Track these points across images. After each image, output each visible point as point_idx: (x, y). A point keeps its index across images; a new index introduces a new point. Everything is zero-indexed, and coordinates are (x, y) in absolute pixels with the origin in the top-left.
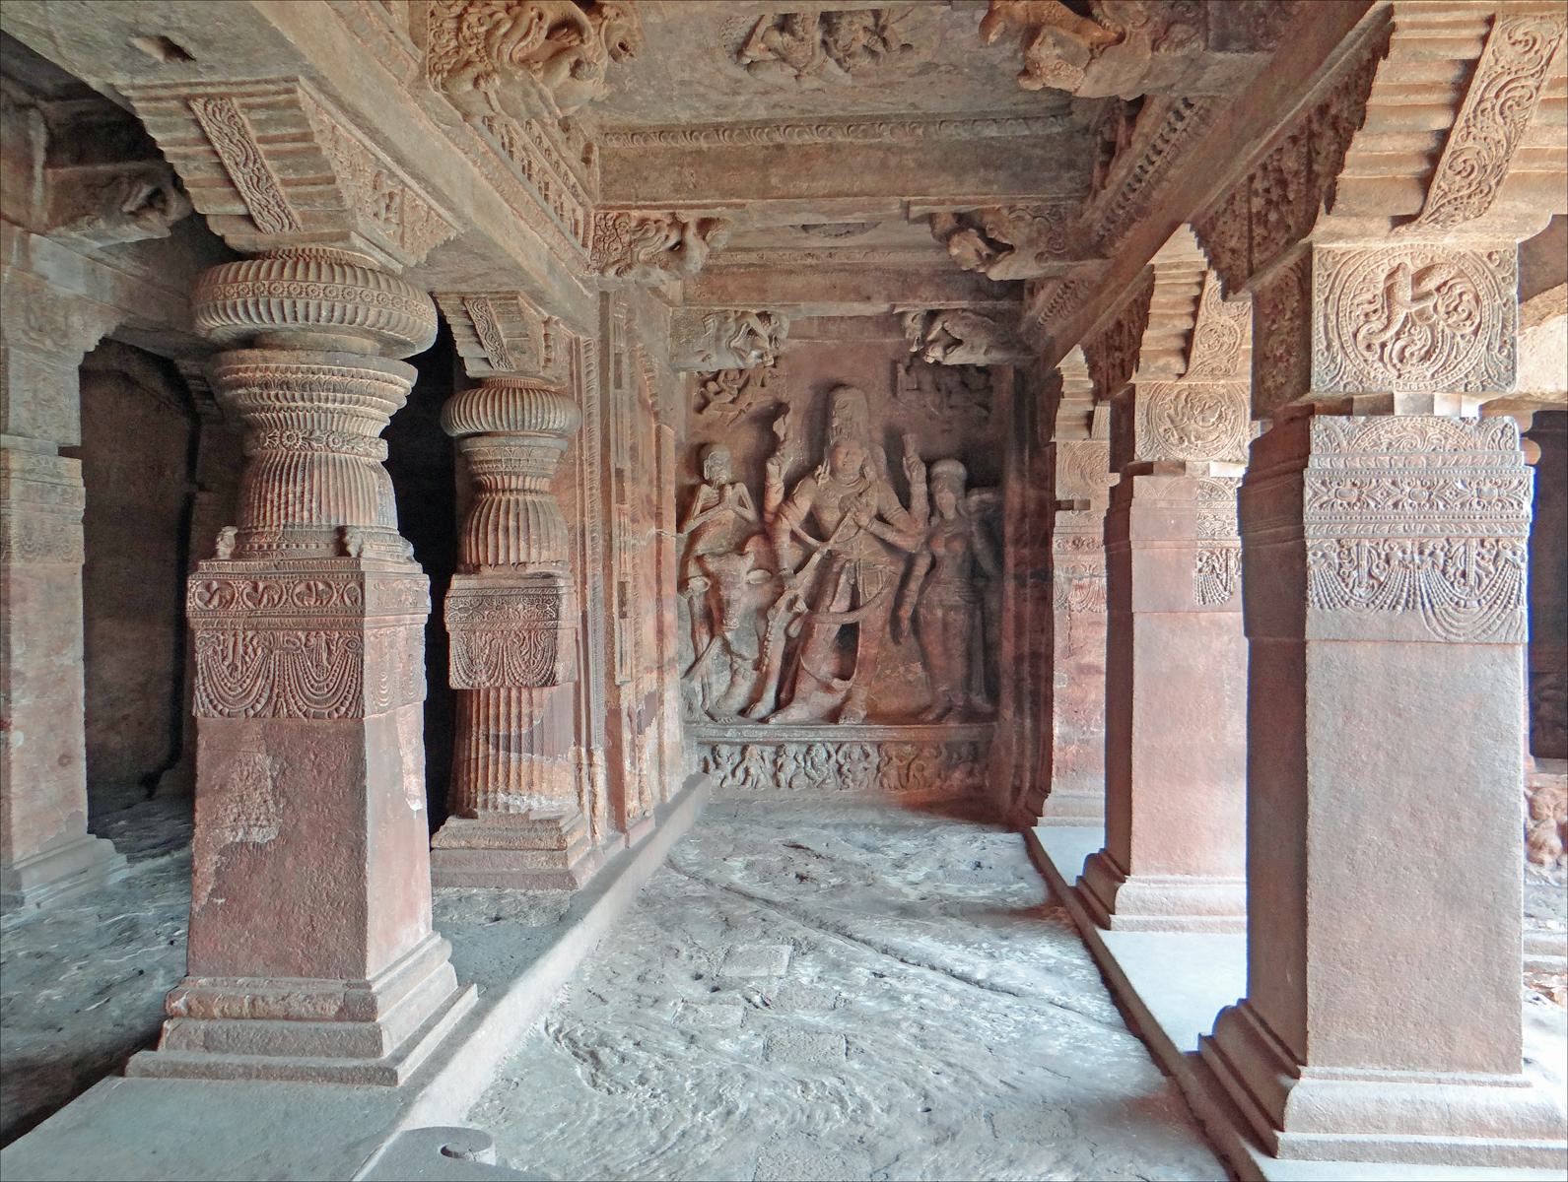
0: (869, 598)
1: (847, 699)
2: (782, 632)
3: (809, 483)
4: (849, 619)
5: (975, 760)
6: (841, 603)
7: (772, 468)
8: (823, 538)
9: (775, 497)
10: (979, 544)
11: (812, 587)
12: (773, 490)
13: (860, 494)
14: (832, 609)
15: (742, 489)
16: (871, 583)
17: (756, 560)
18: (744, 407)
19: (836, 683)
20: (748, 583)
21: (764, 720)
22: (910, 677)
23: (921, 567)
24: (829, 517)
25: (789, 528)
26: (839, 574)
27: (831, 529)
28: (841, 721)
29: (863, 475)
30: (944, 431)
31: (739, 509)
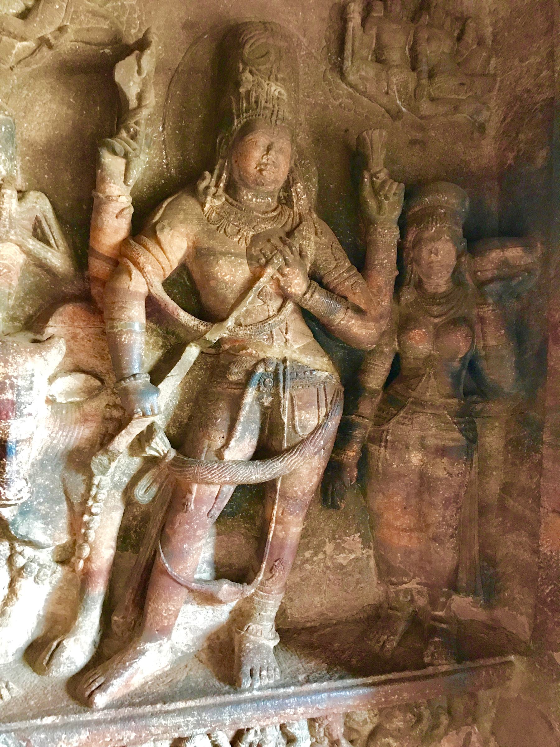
0: (303, 433)
1: (241, 618)
2: (118, 495)
3: (188, 203)
4: (258, 474)
5: (475, 721)
6: (243, 445)
7: (112, 163)
8: (211, 315)
9: (114, 226)
10: (494, 339)
11: (180, 407)
12: (113, 208)
13: (290, 234)
14: (228, 455)
15: (40, 205)
16: (305, 407)
17: (70, 352)
18: (48, 32)
19: (226, 588)
20: (51, 401)
21: (79, 689)
22: (342, 559)
23: (376, 378)
24: (230, 273)
25: (143, 290)
26: (244, 385)
27: (231, 297)
28: (246, 683)
29: (286, 201)
30: (413, 142)
31: (33, 244)
